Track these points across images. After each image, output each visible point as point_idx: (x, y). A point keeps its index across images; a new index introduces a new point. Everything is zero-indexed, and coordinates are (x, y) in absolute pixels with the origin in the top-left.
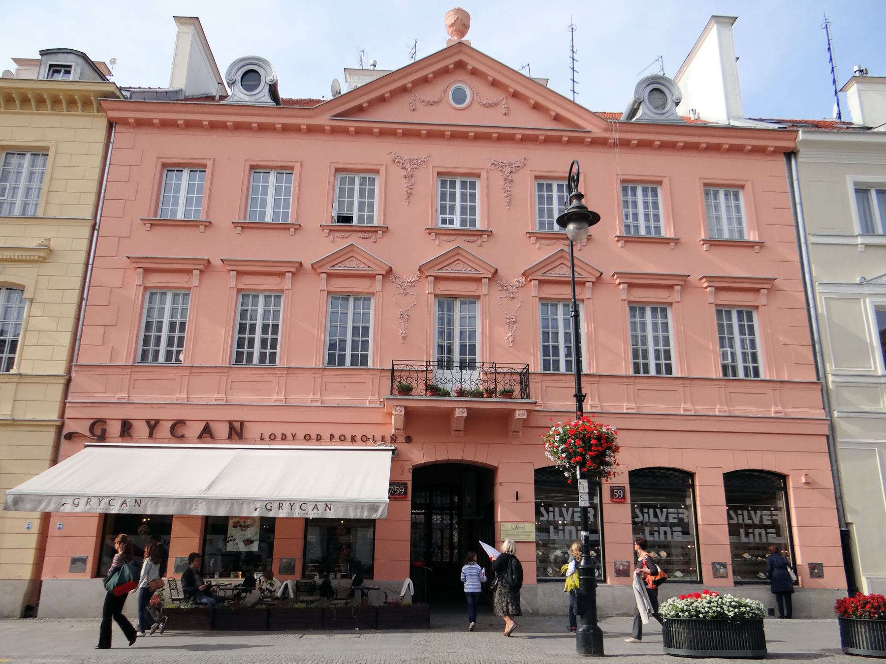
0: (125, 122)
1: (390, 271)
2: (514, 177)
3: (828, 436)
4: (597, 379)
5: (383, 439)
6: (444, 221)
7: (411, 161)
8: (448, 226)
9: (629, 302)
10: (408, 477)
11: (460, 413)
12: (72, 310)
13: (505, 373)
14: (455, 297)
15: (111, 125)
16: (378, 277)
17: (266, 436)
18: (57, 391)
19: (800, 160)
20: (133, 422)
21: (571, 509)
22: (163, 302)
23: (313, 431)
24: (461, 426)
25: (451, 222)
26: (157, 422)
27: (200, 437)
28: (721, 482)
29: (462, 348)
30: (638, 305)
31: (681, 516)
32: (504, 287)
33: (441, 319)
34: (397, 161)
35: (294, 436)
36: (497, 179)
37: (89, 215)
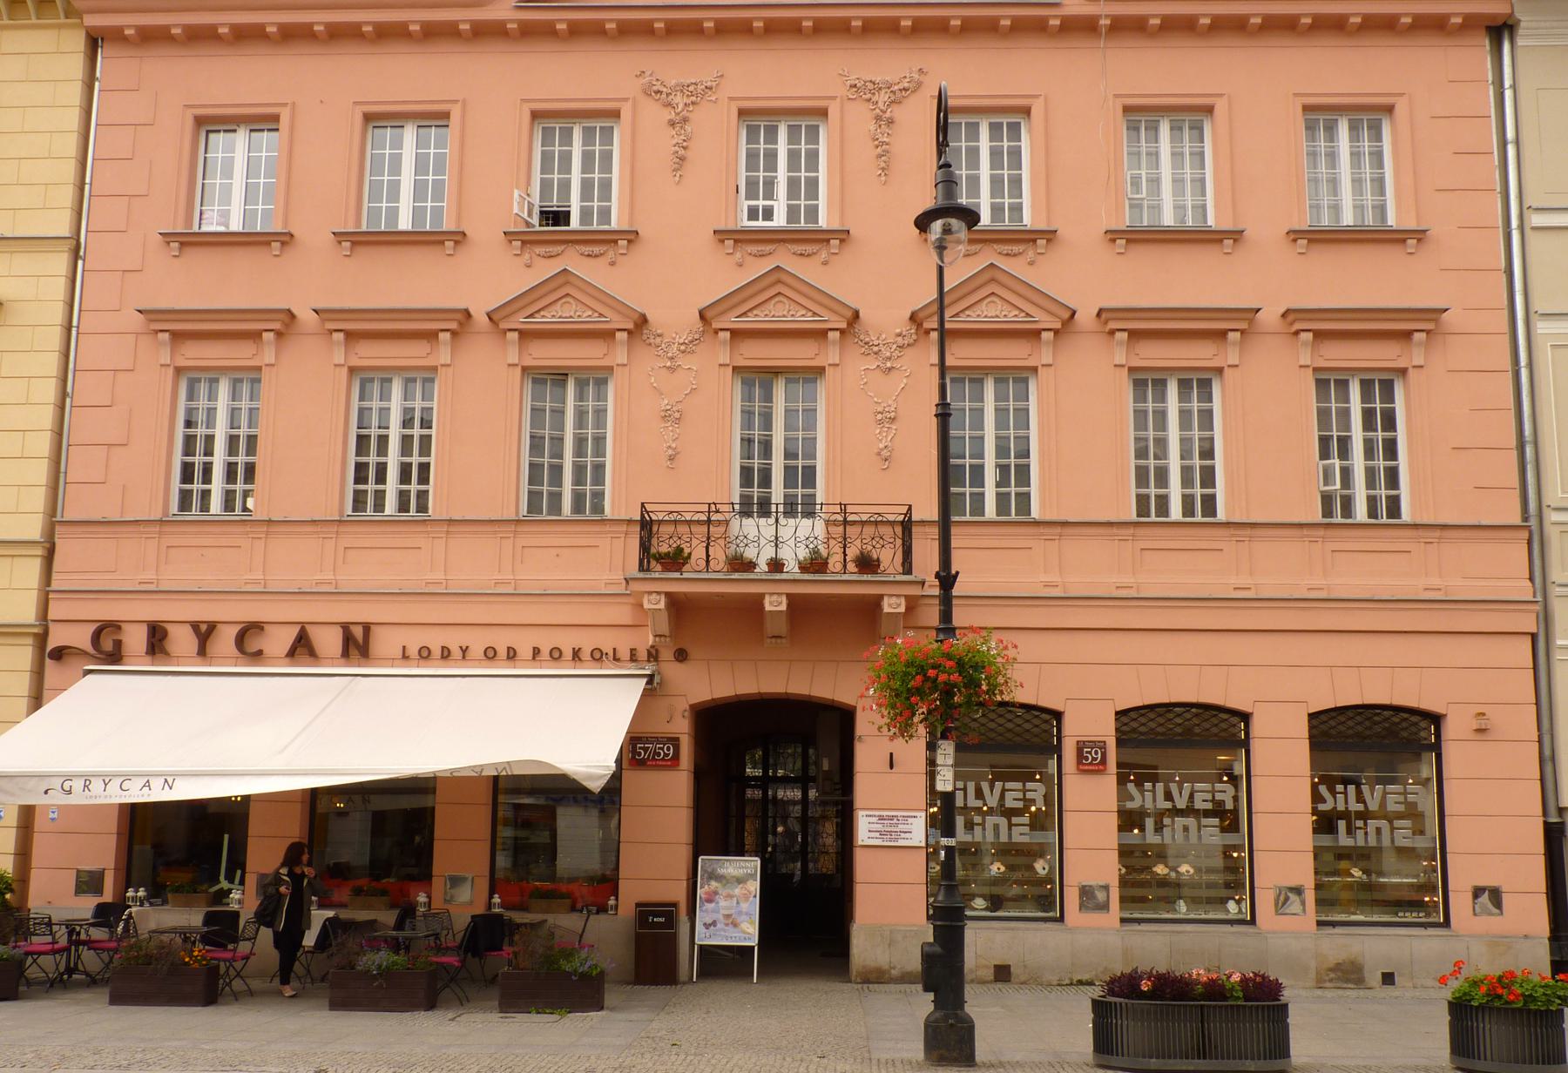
0: (116, 36)
1: (643, 321)
2: (896, 112)
3: (1534, 637)
4: (1058, 530)
5: (633, 657)
6: (753, 213)
7: (682, 88)
8: (761, 223)
9: (1131, 370)
10: (682, 728)
11: (775, 604)
12: (47, 417)
13: (863, 523)
14: (776, 372)
15: (94, 42)
16: (618, 334)
17: (413, 652)
18: (31, 570)
19: (1520, 42)
20: (169, 627)
21: (998, 785)
22: (212, 396)
23: (502, 641)
24: (782, 627)
25: (768, 213)
26: (212, 626)
27: (292, 653)
28: (1303, 729)
29: (790, 472)
30: (1150, 376)
31: (1219, 797)
32: (870, 349)
33: (747, 414)
34: (651, 92)
35: (464, 651)
36: (860, 119)
37: (64, 230)
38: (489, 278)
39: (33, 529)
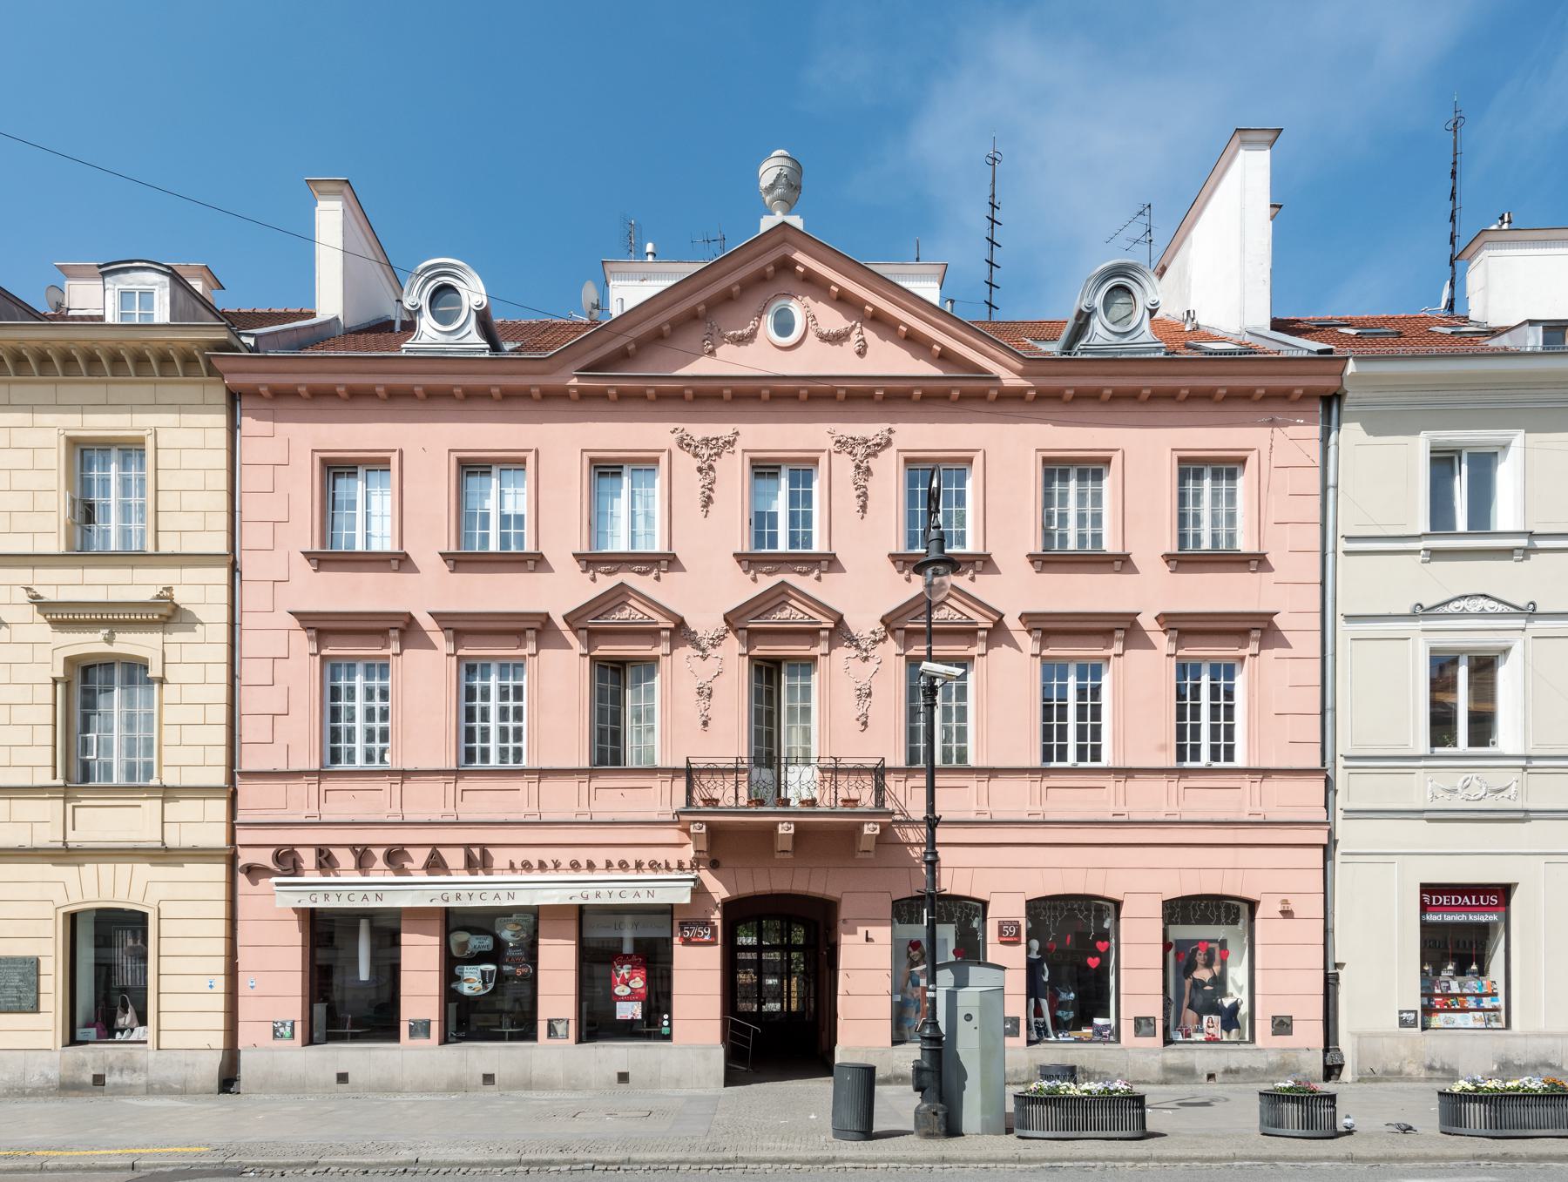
0: (254, 393)
2: (872, 462)
3: (1325, 847)
5: (680, 866)
7: (706, 442)
12: (222, 693)
15: (234, 398)
18: (219, 807)
19: (1345, 409)
36: (844, 466)
37: (221, 547)
38: (561, 591)
39: (218, 778)
